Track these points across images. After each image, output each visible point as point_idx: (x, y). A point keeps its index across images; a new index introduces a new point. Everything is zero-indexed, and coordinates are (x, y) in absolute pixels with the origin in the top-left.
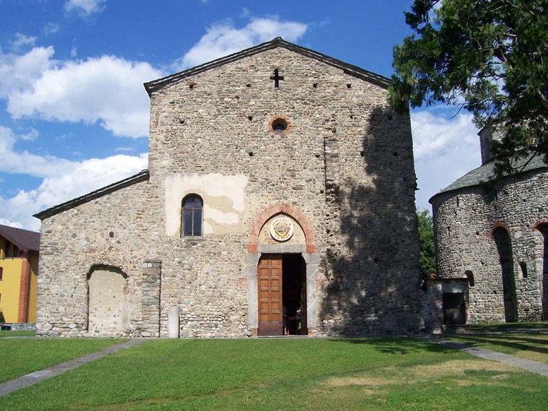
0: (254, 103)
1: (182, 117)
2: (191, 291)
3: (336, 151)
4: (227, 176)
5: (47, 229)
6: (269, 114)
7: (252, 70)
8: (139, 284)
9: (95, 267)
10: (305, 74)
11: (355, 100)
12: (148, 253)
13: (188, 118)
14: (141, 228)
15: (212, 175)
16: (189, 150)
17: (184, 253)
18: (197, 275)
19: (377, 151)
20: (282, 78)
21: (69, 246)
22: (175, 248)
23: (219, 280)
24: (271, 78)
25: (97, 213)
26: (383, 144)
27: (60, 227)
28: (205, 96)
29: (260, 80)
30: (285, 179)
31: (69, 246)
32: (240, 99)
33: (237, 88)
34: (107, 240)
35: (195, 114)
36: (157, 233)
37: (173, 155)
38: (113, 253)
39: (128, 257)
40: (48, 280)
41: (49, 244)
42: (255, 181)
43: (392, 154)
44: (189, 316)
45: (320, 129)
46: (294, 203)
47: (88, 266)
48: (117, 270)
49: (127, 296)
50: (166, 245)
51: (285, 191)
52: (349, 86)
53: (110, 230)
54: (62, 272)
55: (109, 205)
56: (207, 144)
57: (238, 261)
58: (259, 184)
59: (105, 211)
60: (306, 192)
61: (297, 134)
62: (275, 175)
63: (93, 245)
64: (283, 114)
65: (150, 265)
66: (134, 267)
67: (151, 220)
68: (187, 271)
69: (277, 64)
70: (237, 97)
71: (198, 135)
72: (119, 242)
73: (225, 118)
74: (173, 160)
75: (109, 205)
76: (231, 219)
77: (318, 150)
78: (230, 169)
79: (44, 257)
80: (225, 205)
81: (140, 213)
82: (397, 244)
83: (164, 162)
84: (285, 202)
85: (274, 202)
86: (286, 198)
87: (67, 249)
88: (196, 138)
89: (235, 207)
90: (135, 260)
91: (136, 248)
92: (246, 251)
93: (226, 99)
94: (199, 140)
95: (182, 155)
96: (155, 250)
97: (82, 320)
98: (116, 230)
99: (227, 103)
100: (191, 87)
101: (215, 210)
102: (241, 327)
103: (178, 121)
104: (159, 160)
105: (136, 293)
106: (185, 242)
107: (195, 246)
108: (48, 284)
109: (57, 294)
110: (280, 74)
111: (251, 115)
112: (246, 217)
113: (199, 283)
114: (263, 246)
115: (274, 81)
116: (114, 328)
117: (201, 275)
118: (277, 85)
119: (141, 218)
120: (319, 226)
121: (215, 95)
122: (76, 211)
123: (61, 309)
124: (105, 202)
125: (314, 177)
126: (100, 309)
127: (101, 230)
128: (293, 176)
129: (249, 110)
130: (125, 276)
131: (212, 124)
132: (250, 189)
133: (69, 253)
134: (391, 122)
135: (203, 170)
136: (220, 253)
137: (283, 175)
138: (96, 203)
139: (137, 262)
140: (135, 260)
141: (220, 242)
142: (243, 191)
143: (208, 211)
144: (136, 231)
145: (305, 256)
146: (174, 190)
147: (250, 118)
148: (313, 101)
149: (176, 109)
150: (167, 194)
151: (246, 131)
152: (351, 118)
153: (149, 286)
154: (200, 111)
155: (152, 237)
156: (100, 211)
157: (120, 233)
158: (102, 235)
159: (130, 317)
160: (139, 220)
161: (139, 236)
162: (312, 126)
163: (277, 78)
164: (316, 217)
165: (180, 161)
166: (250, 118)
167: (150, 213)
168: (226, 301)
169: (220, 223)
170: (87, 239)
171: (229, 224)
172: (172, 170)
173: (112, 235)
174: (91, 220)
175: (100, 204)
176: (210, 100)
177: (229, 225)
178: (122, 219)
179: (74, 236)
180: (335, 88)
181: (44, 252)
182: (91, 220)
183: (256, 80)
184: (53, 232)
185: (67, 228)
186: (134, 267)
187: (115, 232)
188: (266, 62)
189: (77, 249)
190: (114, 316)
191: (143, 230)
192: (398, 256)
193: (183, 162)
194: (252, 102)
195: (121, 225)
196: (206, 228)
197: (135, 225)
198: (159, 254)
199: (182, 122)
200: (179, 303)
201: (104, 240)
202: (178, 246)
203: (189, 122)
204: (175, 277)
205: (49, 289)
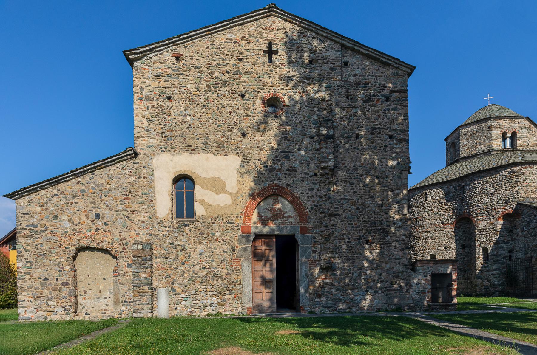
0: (246, 79)
2: (184, 272)
4: (219, 157)
5: (23, 211)
6: (262, 91)
7: (244, 42)
8: (129, 266)
9: (80, 249)
10: (301, 48)
11: (352, 79)
12: (138, 234)
13: (176, 94)
14: (128, 210)
15: (203, 155)
16: (178, 128)
17: (176, 235)
18: (189, 256)
19: (373, 134)
20: (276, 52)
21: (50, 228)
22: (167, 229)
23: (213, 261)
24: (265, 52)
25: (79, 193)
26: (379, 126)
27: (39, 209)
28: (193, 69)
29: (253, 54)
30: (278, 160)
31: (50, 228)
32: (231, 74)
33: (228, 62)
34: (93, 221)
35: (183, 90)
36: (148, 214)
38: (100, 235)
39: (117, 237)
40: (29, 265)
41: (27, 226)
42: (248, 162)
43: (388, 137)
44: (183, 296)
45: (315, 109)
46: (288, 185)
47: (73, 248)
48: (107, 251)
49: (117, 278)
50: (157, 226)
51: (279, 173)
52: (346, 64)
53: (95, 211)
54: (44, 255)
55: (93, 185)
56: (198, 123)
57: (232, 242)
59: (89, 191)
60: (300, 175)
61: (291, 114)
63: (77, 227)
65: (140, 247)
66: (124, 249)
67: (140, 201)
68: (179, 253)
69: (270, 36)
70: (228, 72)
71: (188, 112)
72: (105, 224)
73: (215, 95)
74: (161, 138)
75: (93, 185)
76: (223, 200)
77: (313, 131)
78: (222, 149)
79: (22, 240)
80: (217, 185)
81: (127, 193)
83: (151, 140)
86: (279, 179)
87: (48, 231)
88: (185, 116)
89: (228, 188)
90: (124, 242)
91: (125, 230)
93: (216, 74)
94: (189, 118)
95: (170, 134)
96: (145, 232)
97: (70, 304)
98: (104, 211)
99: (217, 78)
101: (207, 191)
102: (235, 305)
103: (165, 96)
104: (146, 139)
105: (127, 274)
106: (177, 223)
107: (187, 228)
108: (28, 268)
109: (40, 278)
110: (274, 47)
111: (243, 92)
112: (240, 199)
113: (192, 263)
115: (267, 55)
116: (105, 310)
117: (195, 257)
118: (270, 60)
119: (128, 199)
120: (312, 208)
121: (204, 69)
122: (55, 192)
123: (46, 293)
124: (88, 182)
125: (308, 159)
126: (90, 292)
127: (85, 211)
128: (287, 157)
129: (241, 86)
130: (114, 257)
131: (202, 100)
132: (243, 170)
133: (50, 236)
134: (388, 103)
135: (193, 150)
137: (276, 157)
138: (78, 183)
139: (126, 244)
140: (124, 242)
141: (213, 223)
142: (236, 172)
143: (200, 192)
144: (124, 213)
145: (299, 237)
146: (164, 168)
147: (243, 96)
150: (155, 174)
151: (238, 109)
152: (347, 98)
153: (139, 268)
154: (188, 86)
155: (142, 219)
156: (83, 191)
157: (108, 215)
158: (87, 217)
159: (121, 299)
160: (126, 201)
161: (128, 217)
162: (306, 106)
164: (310, 199)
165: (168, 139)
166: (243, 96)
167: (139, 192)
168: (220, 281)
169: (211, 203)
171: (222, 205)
173: (98, 216)
174: (72, 200)
175: (83, 184)
176: (199, 74)
177: (221, 207)
178: (109, 200)
179: (55, 217)
180: (332, 66)
181: (22, 234)
182: (72, 200)
183: (248, 54)
184: (31, 214)
185: (47, 209)
186: (124, 249)
187: (101, 213)
188: (260, 33)
189: (60, 232)
190: (106, 298)
191: (131, 211)
192: (389, 237)
193: (172, 141)
194: (244, 78)
195: (107, 206)
196: (199, 210)
197: (123, 206)
198: (151, 235)
199: (169, 98)
200: (173, 284)
201: (89, 222)
202: (169, 227)
203: (176, 97)
204: (167, 258)
205: (30, 273)
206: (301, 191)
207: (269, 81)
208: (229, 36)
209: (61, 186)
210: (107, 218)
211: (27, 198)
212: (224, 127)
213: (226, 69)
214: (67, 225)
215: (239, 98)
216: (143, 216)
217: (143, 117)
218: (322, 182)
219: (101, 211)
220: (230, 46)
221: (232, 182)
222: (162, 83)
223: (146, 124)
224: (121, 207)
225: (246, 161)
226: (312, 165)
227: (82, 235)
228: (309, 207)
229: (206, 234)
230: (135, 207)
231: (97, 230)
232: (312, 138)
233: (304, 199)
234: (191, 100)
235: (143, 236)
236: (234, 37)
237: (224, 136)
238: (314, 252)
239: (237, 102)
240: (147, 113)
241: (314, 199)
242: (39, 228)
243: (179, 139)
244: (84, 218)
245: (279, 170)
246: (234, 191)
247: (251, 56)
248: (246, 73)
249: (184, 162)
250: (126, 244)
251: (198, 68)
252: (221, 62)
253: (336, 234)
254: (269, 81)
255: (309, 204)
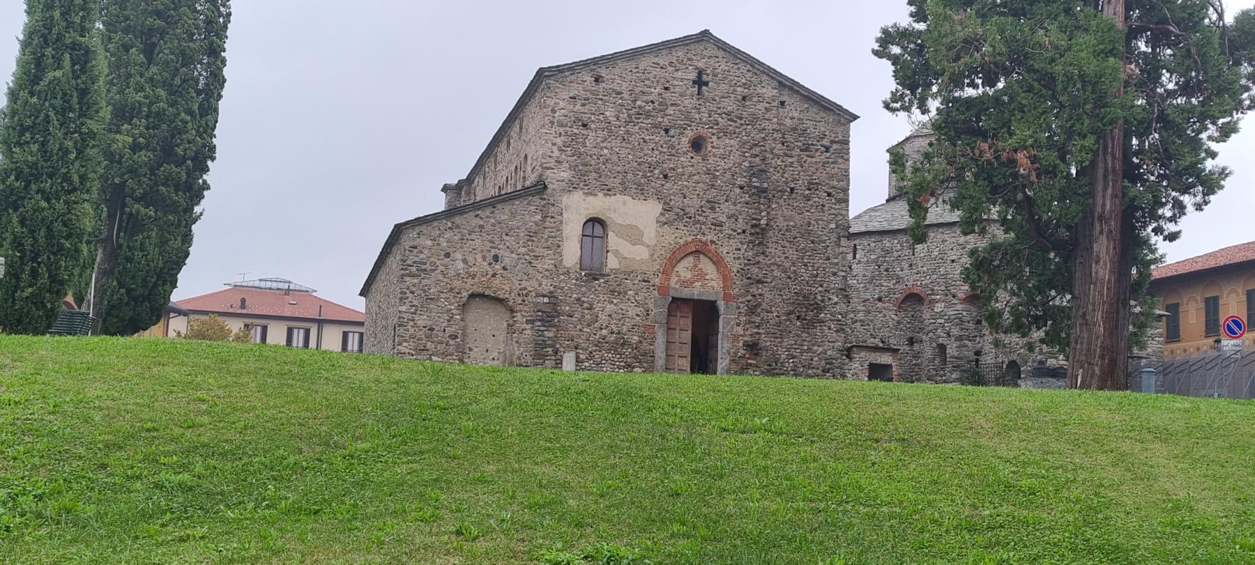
1: (585, 118)
3: (765, 185)
9: (473, 296)
12: (540, 285)
16: (593, 163)
20: (706, 84)
24: (694, 82)
27: (429, 243)
37: (573, 167)
38: (497, 282)
46: (712, 242)
48: (501, 301)
53: (493, 252)
56: (615, 158)
58: (672, 215)
59: (488, 227)
62: (693, 203)
64: (704, 131)
69: (701, 65)
70: (653, 102)
72: (504, 268)
76: (639, 254)
78: (641, 192)
80: (634, 235)
82: (823, 301)
84: (704, 239)
85: (690, 239)
88: (602, 149)
89: (646, 239)
92: (656, 292)
93: (639, 103)
94: (606, 151)
96: (549, 282)
99: (640, 107)
100: (597, 80)
101: (621, 241)
114: (676, 290)
117: (603, 318)
121: (626, 96)
122: (450, 224)
128: (713, 209)
130: (512, 311)
132: (663, 219)
133: (440, 277)
136: (626, 293)
139: (527, 295)
145: (721, 305)
147: (667, 131)
148: (741, 119)
149: (578, 107)
150: (565, 215)
156: (481, 227)
158: (484, 258)
163: (700, 82)
166: (667, 131)
167: (546, 233)
170: (465, 261)
172: (572, 187)
173: (496, 258)
179: (447, 255)
183: (676, 83)
184: (420, 248)
194: (670, 111)
196: (612, 263)
199: (584, 125)
203: (593, 126)
206: (728, 250)
207: (697, 116)
208: (656, 60)
209: (457, 220)
210: (507, 261)
211: (417, 229)
212: (645, 167)
213: (650, 98)
214: (460, 265)
215: (663, 133)
216: (548, 263)
217: (554, 144)
218: (751, 242)
219: (501, 253)
220: (657, 72)
221: (650, 231)
222: (578, 107)
223: (556, 153)
224: (523, 250)
225: (667, 209)
226: (740, 220)
227: (476, 280)
228: (735, 270)
229: (616, 292)
230: (540, 251)
231: (494, 275)
232: (741, 188)
233: (729, 259)
234: (610, 131)
235: (547, 287)
236: (662, 62)
237: (644, 176)
238: (738, 325)
239: (659, 138)
240: (559, 141)
241: (742, 261)
242: (428, 267)
243: (594, 175)
244: (479, 259)
245: (704, 223)
246: (653, 243)
247: (679, 86)
248: (672, 105)
249: (597, 204)
250: (527, 295)
251: (619, 93)
252: (646, 89)
253: (764, 306)
254: (697, 116)
255: (735, 266)
